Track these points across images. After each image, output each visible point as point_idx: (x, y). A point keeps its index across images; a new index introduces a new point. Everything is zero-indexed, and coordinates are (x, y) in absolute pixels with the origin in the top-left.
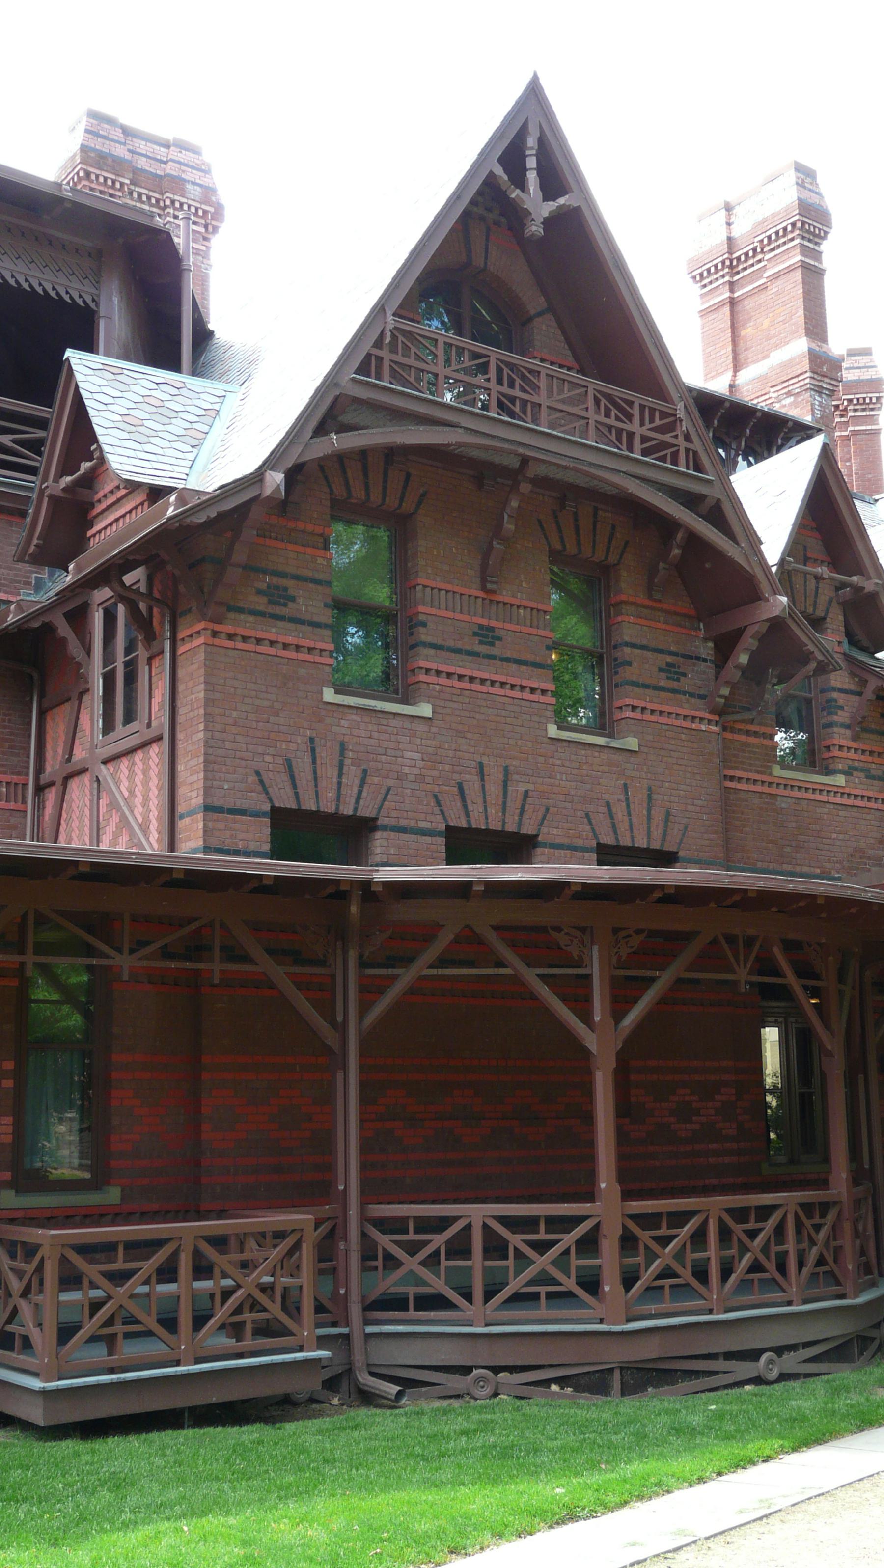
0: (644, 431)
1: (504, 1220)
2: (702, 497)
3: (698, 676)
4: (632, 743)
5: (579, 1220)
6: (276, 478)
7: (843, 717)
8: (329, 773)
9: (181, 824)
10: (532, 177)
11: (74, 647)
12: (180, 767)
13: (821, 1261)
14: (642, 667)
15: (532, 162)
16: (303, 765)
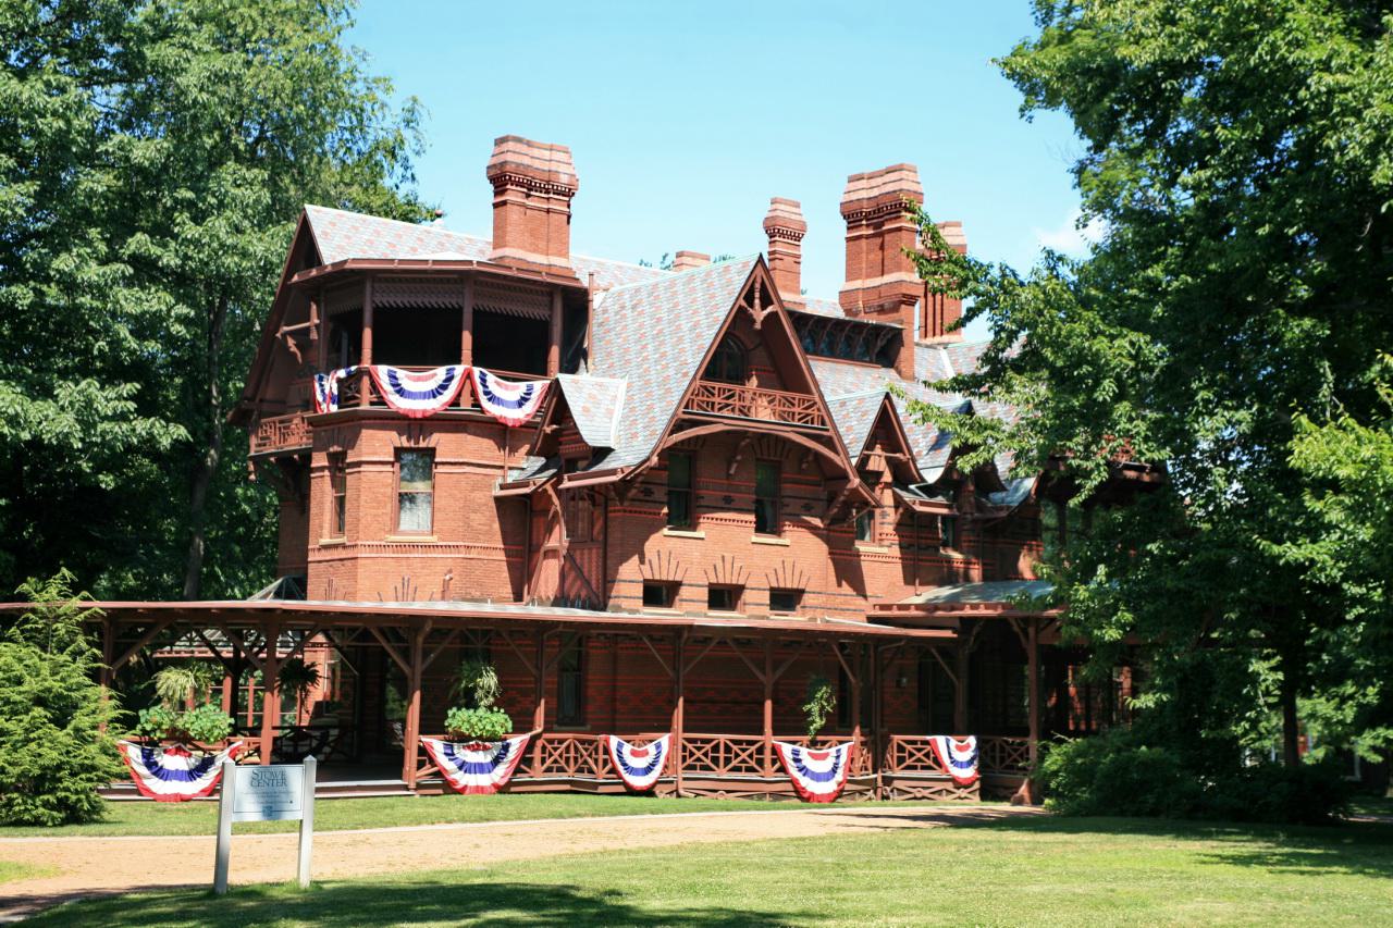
0: (799, 410)
1: (731, 741)
2: (823, 436)
5: (756, 742)
6: (655, 459)
8: (664, 563)
10: (757, 301)
12: (609, 562)
15: (757, 295)
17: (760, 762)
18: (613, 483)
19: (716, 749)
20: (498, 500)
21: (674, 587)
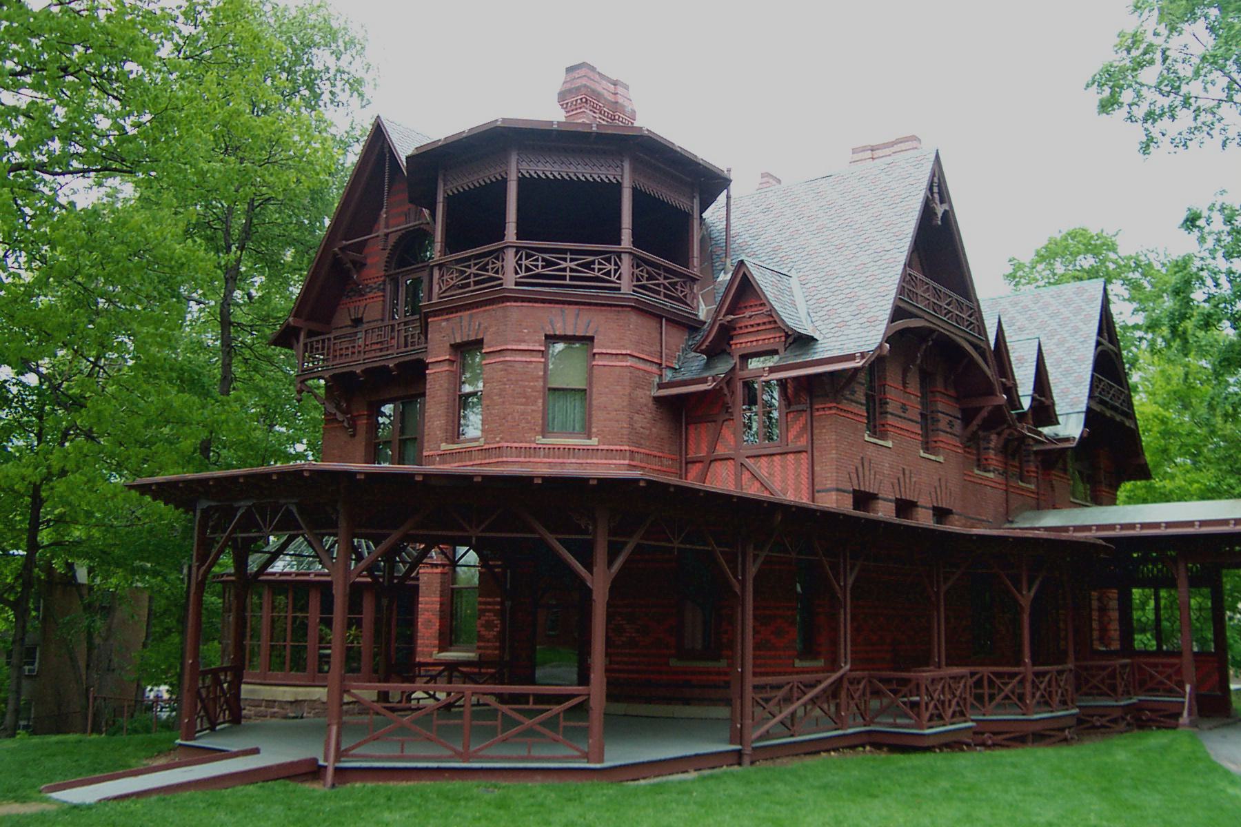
1: (993, 673)
3: (958, 424)
4: (941, 459)
7: (992, 445)
9: (817, 495)
10: (936, 196)
11: (728, 399)
13: (1043, 696)
14: (943, 425)
15: (936, 190)
16: (860, 469)
17: (1021, 698)
18: (856, 370)
19: (979, 684)
20: (658, 400)
21: (874, 497)
